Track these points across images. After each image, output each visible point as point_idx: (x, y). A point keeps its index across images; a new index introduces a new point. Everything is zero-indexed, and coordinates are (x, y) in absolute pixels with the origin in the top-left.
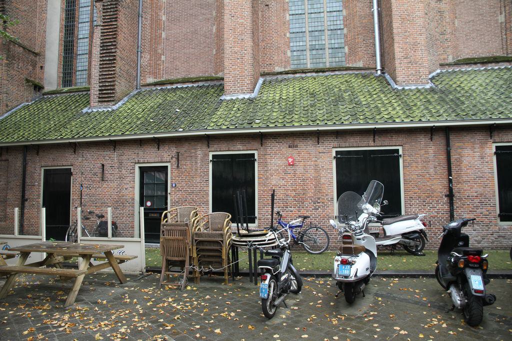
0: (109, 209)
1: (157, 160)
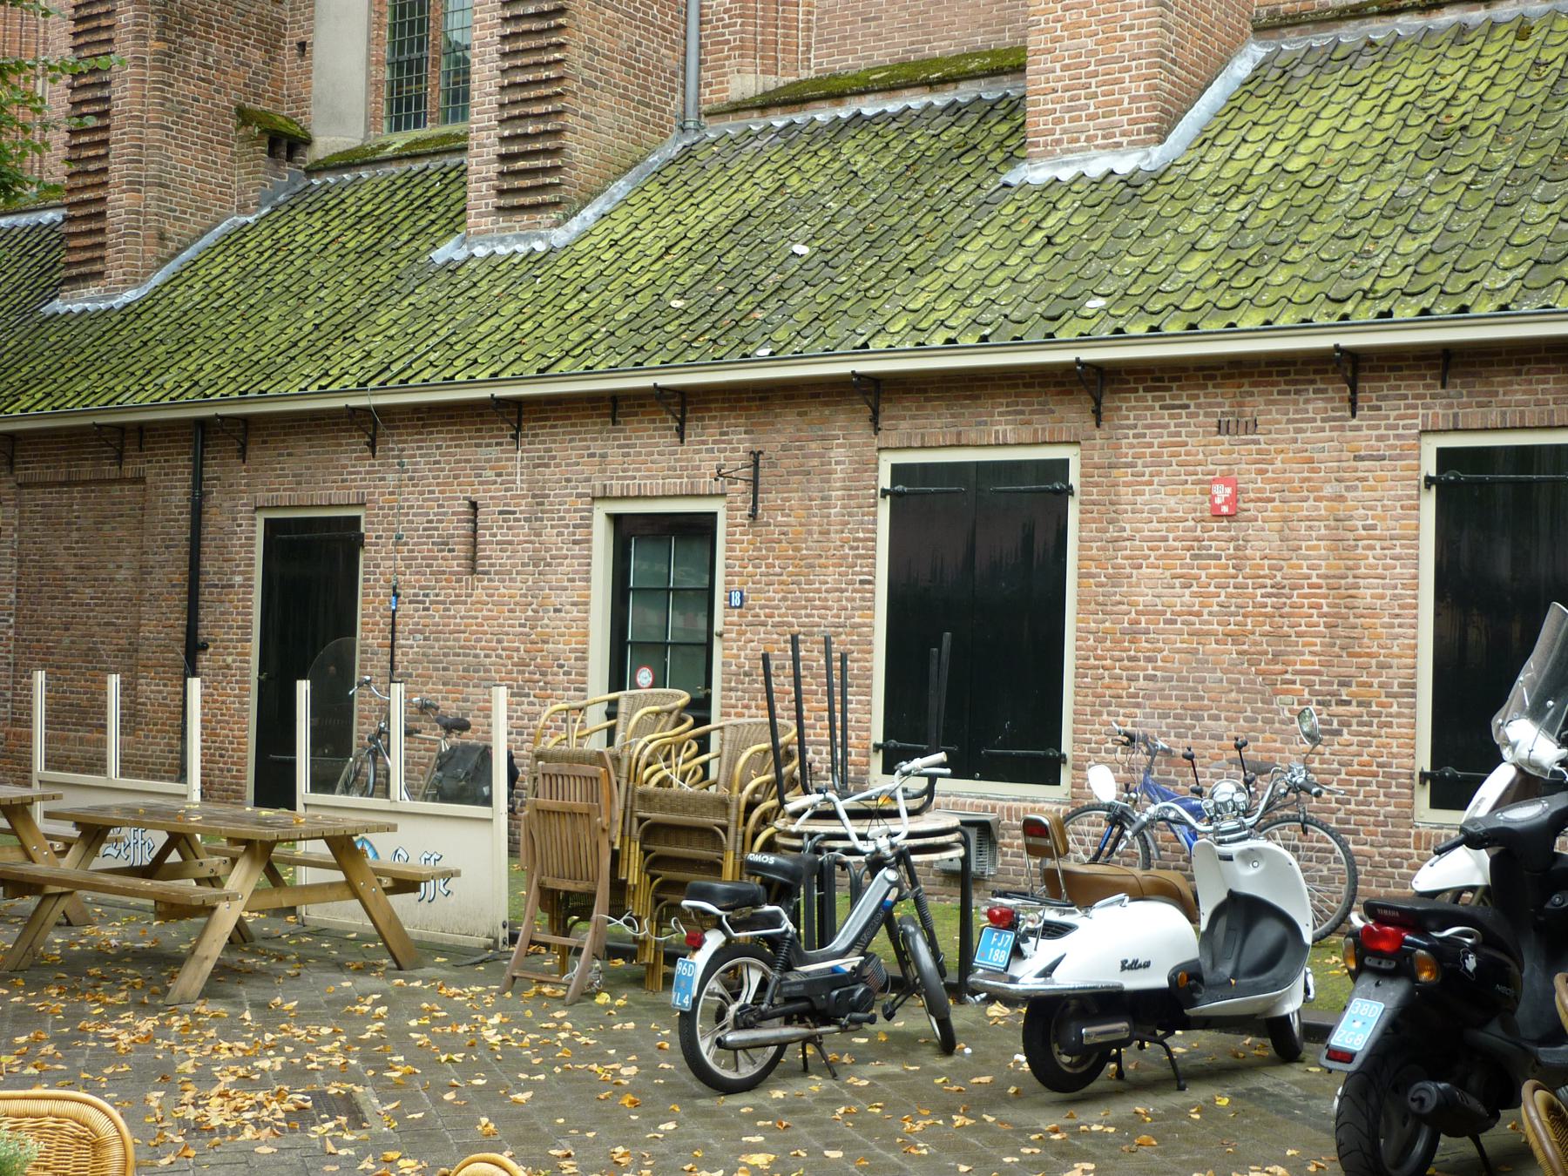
0: (501, 695)
1: (674, 485)
